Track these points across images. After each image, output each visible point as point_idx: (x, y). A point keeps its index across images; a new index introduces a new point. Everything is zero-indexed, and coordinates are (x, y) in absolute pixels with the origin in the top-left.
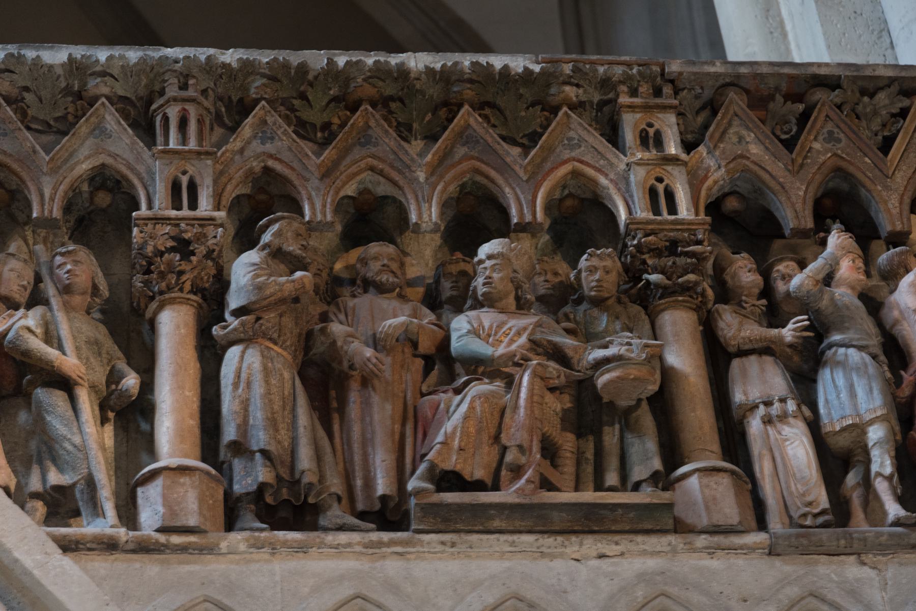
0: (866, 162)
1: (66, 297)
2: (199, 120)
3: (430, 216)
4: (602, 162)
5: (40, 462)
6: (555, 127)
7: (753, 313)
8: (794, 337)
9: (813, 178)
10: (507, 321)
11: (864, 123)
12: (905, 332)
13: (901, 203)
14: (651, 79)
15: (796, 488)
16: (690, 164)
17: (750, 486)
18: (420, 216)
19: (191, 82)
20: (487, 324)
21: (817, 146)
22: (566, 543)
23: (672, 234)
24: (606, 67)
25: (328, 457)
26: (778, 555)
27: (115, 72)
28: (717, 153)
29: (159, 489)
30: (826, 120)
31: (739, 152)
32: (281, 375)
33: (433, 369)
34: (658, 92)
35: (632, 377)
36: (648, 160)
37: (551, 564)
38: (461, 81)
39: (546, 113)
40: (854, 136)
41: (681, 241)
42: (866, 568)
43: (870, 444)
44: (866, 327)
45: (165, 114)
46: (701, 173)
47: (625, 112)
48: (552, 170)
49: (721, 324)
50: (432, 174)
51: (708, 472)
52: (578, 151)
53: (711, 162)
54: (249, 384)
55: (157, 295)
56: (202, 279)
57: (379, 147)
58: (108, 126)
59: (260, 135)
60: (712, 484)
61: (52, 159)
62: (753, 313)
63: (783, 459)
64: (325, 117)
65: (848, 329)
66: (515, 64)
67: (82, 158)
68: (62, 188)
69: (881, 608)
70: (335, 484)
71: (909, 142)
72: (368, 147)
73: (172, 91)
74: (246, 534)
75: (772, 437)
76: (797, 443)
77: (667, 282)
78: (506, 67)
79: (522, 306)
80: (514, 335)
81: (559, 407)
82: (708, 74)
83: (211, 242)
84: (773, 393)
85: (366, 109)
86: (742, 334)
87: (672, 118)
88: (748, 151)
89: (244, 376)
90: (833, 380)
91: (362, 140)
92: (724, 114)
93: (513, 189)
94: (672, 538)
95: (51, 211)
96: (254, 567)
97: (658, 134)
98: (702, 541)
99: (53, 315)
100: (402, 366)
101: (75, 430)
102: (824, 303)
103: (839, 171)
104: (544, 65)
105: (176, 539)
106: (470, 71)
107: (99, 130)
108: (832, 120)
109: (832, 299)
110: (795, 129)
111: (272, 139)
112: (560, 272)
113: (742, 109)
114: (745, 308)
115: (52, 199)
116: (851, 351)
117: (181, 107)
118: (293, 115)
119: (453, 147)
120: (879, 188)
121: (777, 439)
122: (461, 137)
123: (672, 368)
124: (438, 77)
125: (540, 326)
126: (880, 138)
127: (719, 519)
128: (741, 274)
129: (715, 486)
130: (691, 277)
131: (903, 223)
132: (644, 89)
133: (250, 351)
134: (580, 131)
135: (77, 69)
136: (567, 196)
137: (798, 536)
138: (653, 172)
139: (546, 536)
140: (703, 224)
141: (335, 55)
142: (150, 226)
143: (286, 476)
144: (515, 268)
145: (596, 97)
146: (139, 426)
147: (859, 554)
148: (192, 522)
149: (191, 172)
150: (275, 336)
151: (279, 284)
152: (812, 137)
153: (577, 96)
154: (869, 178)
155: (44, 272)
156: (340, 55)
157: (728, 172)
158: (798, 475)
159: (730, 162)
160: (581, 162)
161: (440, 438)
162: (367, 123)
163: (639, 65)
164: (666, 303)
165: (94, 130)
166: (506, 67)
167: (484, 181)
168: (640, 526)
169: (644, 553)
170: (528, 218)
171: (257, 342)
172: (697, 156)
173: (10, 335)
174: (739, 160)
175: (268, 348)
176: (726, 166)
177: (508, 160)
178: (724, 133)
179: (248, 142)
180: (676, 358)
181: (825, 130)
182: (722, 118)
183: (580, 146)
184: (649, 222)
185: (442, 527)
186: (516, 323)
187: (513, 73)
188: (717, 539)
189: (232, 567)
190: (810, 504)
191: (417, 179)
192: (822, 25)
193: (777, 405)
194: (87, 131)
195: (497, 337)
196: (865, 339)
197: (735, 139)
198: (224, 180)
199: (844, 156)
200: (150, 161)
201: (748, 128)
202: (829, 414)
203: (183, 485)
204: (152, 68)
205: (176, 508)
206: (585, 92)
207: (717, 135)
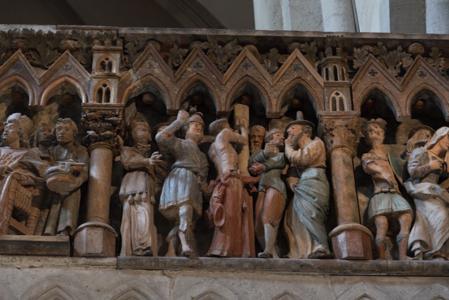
0: (213, 78)
4: (79, 77)
6: (60, 60)
7: (142, 151)
8: (153, 162)
11: (219, 59)
12: (217, 161)
13: (227, 98)
14: (111, 36)
15: (137, 236)
16: (122, 78)
17: (117, 235)
22: (14, 260)
23: (103, 112)
24: (90, 31)
26: (121, 269)
28: (137, 73)
31: (149, 72)
34: (114, 43)
35: (60, 180)
36: (100, 76)
37: (5, 270)
38: (18, 38)
40: (209, 65)
41: (108, 115)
42: (165, 277)
43: (180, 215)
44: (194, 158)
46: (128, 82)
47: (95, 53)
48: (54, 80)
51: (91, 227)
52: (69, 72)
53: (134, 77)
62: (142, 151)
63: (135, 222)
65: (184, 159)
66: (45, 30)
69: (168, 297)
71: (237, 68)
75: (132, 211)
76: (142, 215)
77: (97, 135)
78: (40, 31)
79: (22, 145)
80: (13, 159)
81: (30, 194)
82: (140, 34)
86: (131, 161)
87: (118, 56)
88: (153, 72)
90: (169, 184)
93: (32, 89)
94: (67, 259)
98: (82, 261)
102: (176, 146)
103: (199, 82)
104: (59, 30)
106: (22, 33)
108: (199, 57)
109: (180, 145)
113: (154, 51)
114: (138, 149)
119: (8, 69)
120: (217, 90)
121: (134, 212)
122: (14, 65)
123: (92, 177)
124: (7, 36)
125: (28, 155)
126: (227, 66)
127: (91, 250)
129: (94, 234)
130: (108, 132)
131: (226, 108)
132: (107, 41)
134: (73, 63)
136: (65, 94)
137: (130, 260)
138: (102, 82)
139: (4, 256)
140: (120, 107)
144: (20, 127)
145: (85, 46)
147: (163, 270)
152: (187, 65)
153: (74, 45)
157: (141, 82)
159: (143, 77)
160: (70, 77)
163: (106, 30)
164: (95, 145)
166: (40, 31)
167: (21, 86)
168: (52, 253)
169: (53, 266)
170: (36, 103)
172: (127, 74)
176: (141, 79)
177: (33, 76)
178: (143, 63)
180: (95, 173)
181: (195, 62)
182: (143, 56)
183: (70, 69)
184: (93, 106)
186: (15, 154)
187: (43, 34)
188: (89, 260)
190: (142, 244)
192: (291, 19)
193: (137, 195)
197: (148, 66)
199: (202, 74)
201: (156, 61)
202: (164, 200)
206: (79, 43)
207: (139, 64)
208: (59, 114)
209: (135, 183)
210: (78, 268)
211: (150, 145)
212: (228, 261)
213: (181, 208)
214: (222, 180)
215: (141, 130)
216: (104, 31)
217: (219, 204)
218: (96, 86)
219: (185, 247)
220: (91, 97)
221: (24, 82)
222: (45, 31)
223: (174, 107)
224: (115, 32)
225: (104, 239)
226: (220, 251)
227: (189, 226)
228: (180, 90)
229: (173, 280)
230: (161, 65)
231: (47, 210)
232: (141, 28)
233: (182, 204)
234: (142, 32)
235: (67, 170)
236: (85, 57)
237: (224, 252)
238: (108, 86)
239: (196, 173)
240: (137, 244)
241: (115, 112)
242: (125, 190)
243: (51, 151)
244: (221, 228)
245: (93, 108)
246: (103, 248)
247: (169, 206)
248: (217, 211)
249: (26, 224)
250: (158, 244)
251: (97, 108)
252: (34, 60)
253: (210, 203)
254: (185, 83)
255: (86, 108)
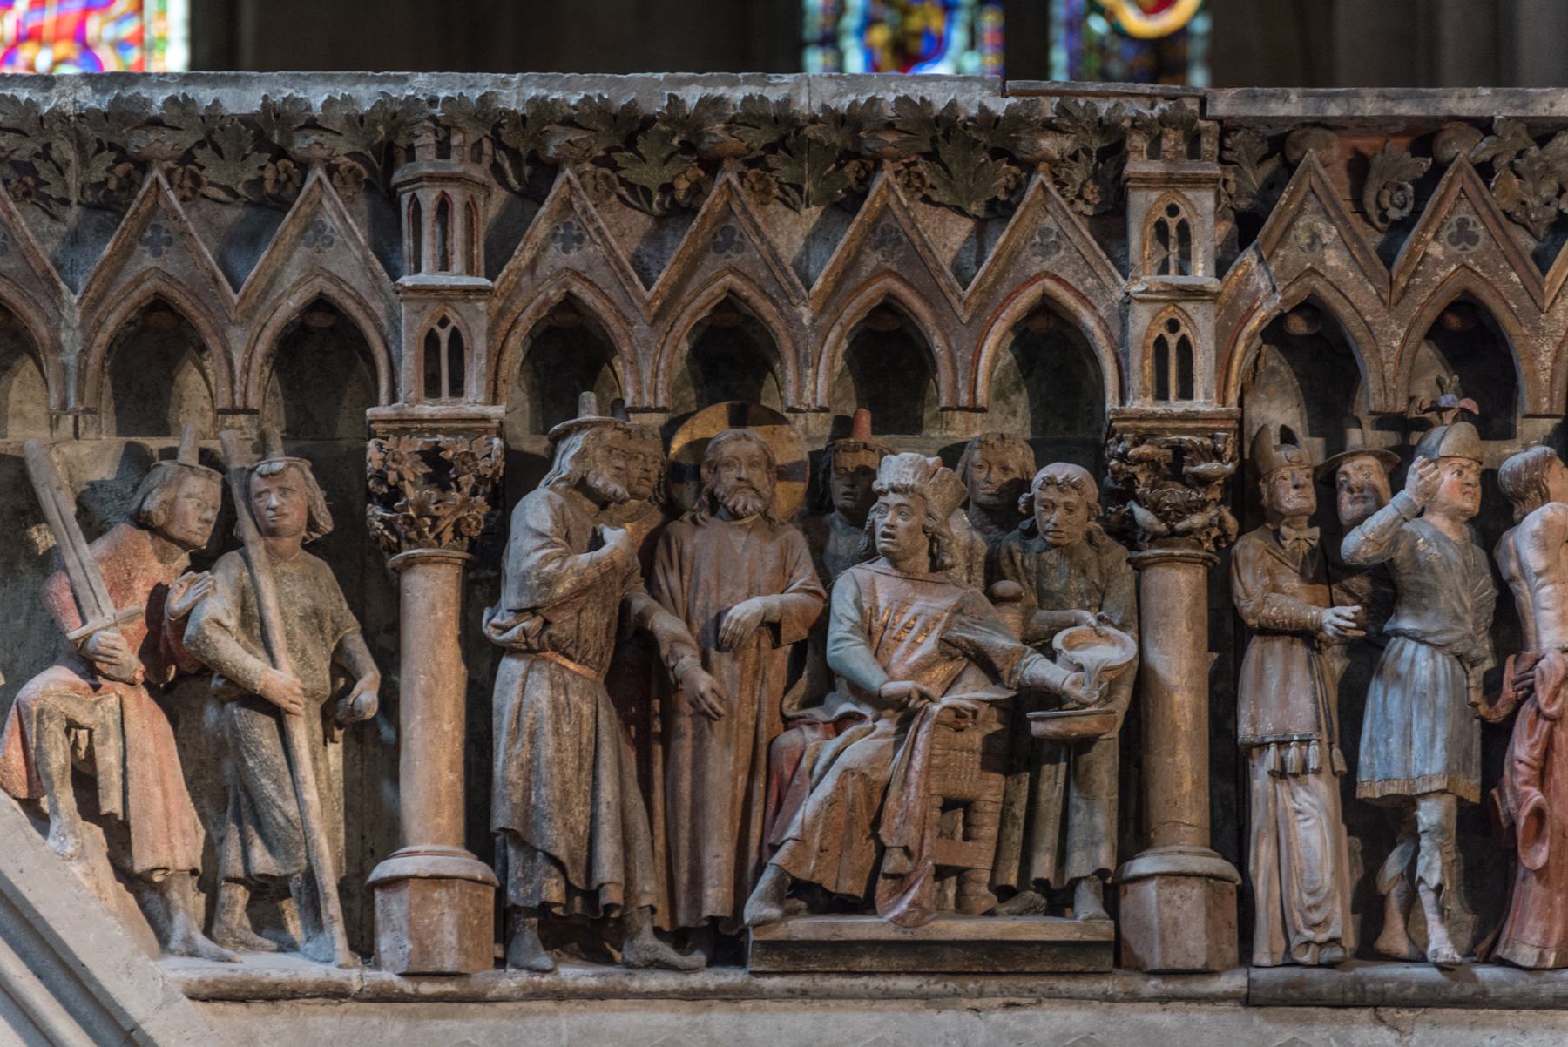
0: (1511, 282)
1: (270, 540)
2: (467, 204)
3: (815, 392)
4: (1089, 282)
5: (239, 821)
7: (1293, 555)
9: (1421, 311)
10: (913, 599)
11: (1529, 185)
17: (1239, 881)
18: (799, 395)
19: (456, 140)
20: (882, 603)
21: (1436, 250)
25: (641, 845)
27: (336, 126)
29: (404, 907)
30: (1459, 198)
32: (579, 714)
33: (800, 676)
36: (1158, 292)
39: (1015, 169)
41: (1191, 451)
43: (1420, 829)
44: (1456, 604)
45: (414, 196)
46: (1243, 304)
48: (1009, 298)
49: (1238, 588)
50: (822, 311)
52: (1054, 258)
54: (533, 736)
55: (404, 544)
56: (469, 525)
57: (745, 254)
58: (327, 221)
59: (562, 231)
60: (1176, 897)
61: (243, 298)
63: (1289, 845)
64: (666, 174)
66: (967, 97)
67: (288, 286)
68: (261, 348)
70: (650, 889)
72: (728, 252)
73: (426, 162)
74: (522, 978)
76: (1310, 823)
80: (920, 633)
83: (482, 464)
84: (1292, 728)
85: (728, 181)
86: (1265, 612)
87: (1205, 200)
88: (1322, 262)
89: (527, 721)
90: (1385, 708)
91: (720, 239)
92: (1292, 194)
93: (946, 337)
95: (245, 395)
96: (533, 1022)
97: (1184, 228)
99: (252, 578)
100: (755, 673)
101: (289, 791)
104: (1012, 100)
105: (427, 988)
107: (313, 231)
109: (1413, 549)
110: (1411, 204)
111: (580, 239)
112: (1012, 466)
115: (247, 371)
116: (1423, 651)
117: (438, 190)
118: (614, 177)
119: (859, 251)
121: (1285, 810)
122: (874, 231)
123: (1154, 672)
126: (1554, 210)
127: (1177, 960)
128: (1281, 492)
129: (1179, 902)
130: (1197, 520)
131: (1551, 400)
133: (534, 676)
135: (277, 116)
139: (933, 980)
141: (680, 83)
142: (392, 439)
143: (577, 879)
145: (1097, 143)
146: (378, 733)
147: (1376, 1007)
148: (449, 965)
149: (453, 323)
150: (571, 650)
151: (579, 573)
152: (1430, 235)
154: (1512, 310)
155: (236, 491)
156: (690, 81)
158: (1306, 876)
160: (1059, 280)
161: (793, 832)
162: (728, 203)
163: (1167, 98)
165: (306, 229)
166: (952, 105)
168: (1065, 967)
171: (544, 658)
172: (1240, 272)
173: (190, 630)
174: (1306, 279)
175: (561, 667)
176: (1284, 292)
177: (942, 281)
178: (1290, 226)
179: (545, 249)
181: (1454, 219)
182: (1289, 202)
183: (1059, 248)
184: (1144, 417)
185: (789, 967)
187: (962, 117)
189: (504, 1022)
190: (1314, 926)
191: (799, 319)
193: (1293, 753)
194: (295, 233)
195: (894, 634)
196: (1451, 630)
197: (1305, 240)
198: (505, 325)
199: (1478, 269)
200: (393, 296)
202: (1372, 764)
203: (438, 902)
204: (394, 116)
205: (428, 942)
207: (1277, 234)
208: (1016, 357)
209: (1284, 702)
210: (1141, 1006)
211: (1316, 531)
212: (1559, 985)
213: (1423, 804)
214: (1542, 696)
215: (1289, 482)
216: (1162, 105)
217: (1535, 796)
218: (1147, 336)
219: (1440, 943)
220: (1135, 382)
221: (917, 304)
222: (968, 102)
223: (1391, 402)
224: (1196, 107)
225: (1209, 915)
226: (1536, 951)
227: (1447, 868)
228: (1408, 334)
229: (1406, 1038)
230: (1347, 238)
231: (1025, 777)
232: (1279, 90)
233: (1424, 795)
234: (1278, 109)
235: (1090, 693)
236: (1095, 177)
237: (1546, 952)
238: (1184, 330)
239: (1459, 657)
240: (1300, 923)
241: (1212, 437)
242: (1254, 722)
243: (1018, 557)
244: (1541, 874)
245: (1144, 425)
246: (1209, 947)
247: (1387, 792)
248: (1530, 815)
249: (967, 824)
250: (1351, 871)
251: (1156, 424)
252: (932, 187)
253: (1507, 773)
254: (1424, 306)
255: (1122, 424)
